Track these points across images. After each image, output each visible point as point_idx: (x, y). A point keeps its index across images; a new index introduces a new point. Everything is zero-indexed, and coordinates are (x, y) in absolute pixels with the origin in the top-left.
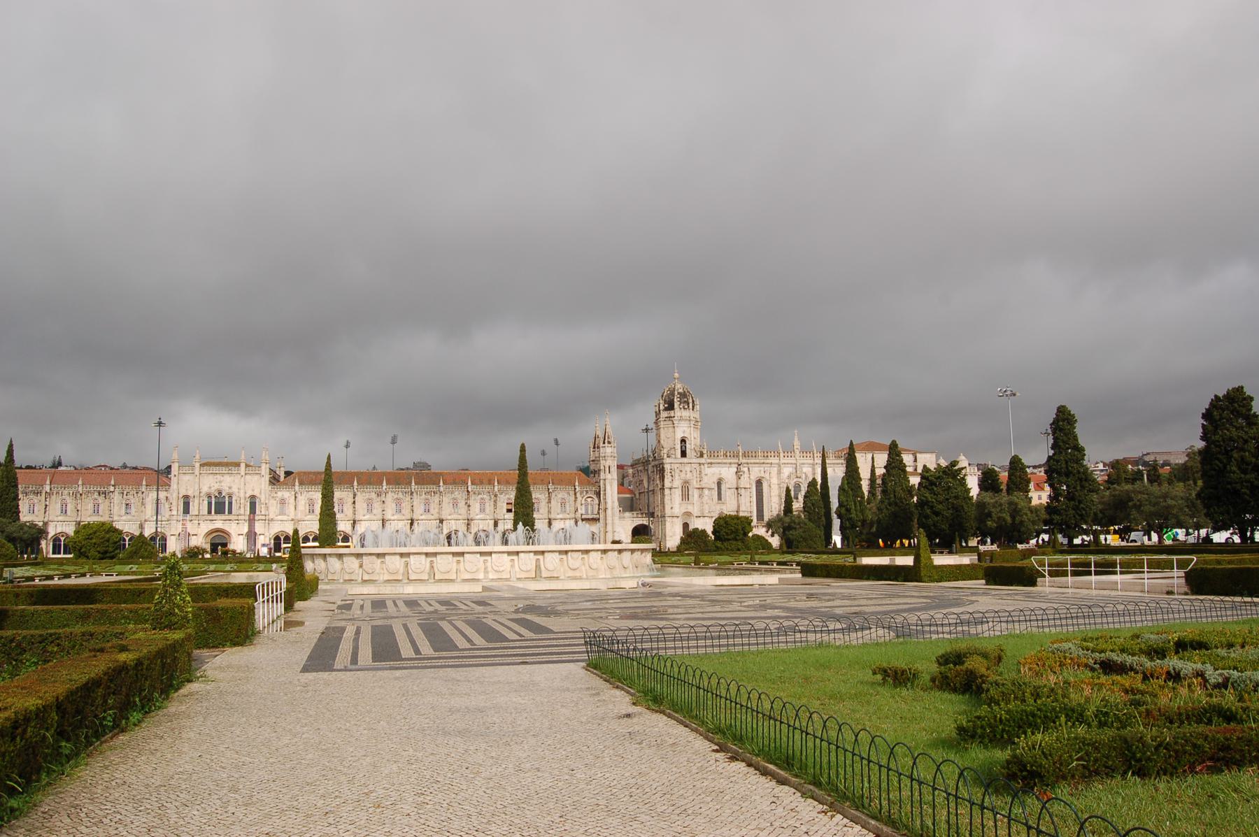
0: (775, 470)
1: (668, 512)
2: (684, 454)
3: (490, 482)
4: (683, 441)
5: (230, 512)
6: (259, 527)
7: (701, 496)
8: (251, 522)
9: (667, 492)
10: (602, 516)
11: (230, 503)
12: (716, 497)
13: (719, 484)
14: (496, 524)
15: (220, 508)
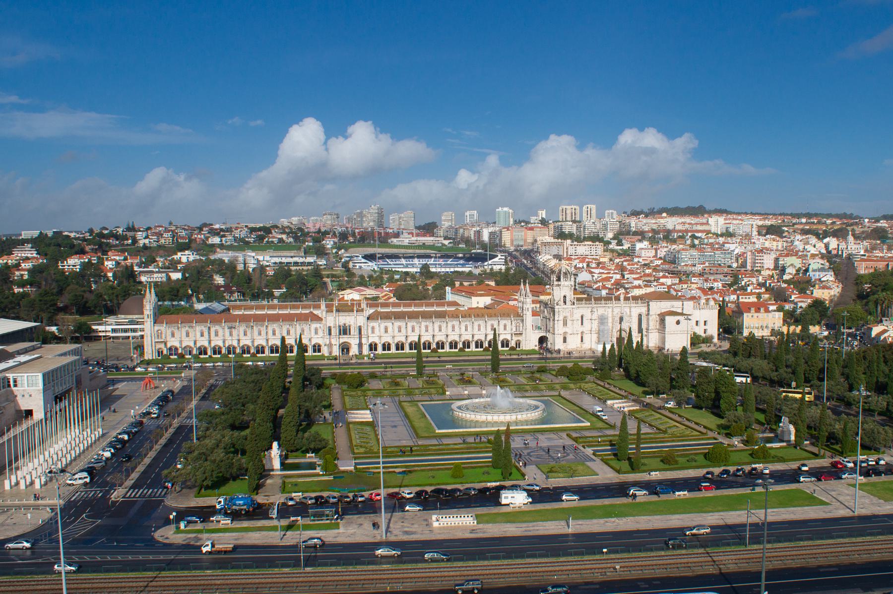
0: (610, 310)
1: (556, 332)
2: (565, 302)
3: (470, 316)
4: (565, 297)
5: (350, 334)
6: (364, 341)
7: (572, 324)
8: (360, 338)
9: (556, 322)
10: (524, 332)
11: (350, 329)
12: (580, 323)
13: (582, 317)
14: (473, 336)
15: (345, 333)
